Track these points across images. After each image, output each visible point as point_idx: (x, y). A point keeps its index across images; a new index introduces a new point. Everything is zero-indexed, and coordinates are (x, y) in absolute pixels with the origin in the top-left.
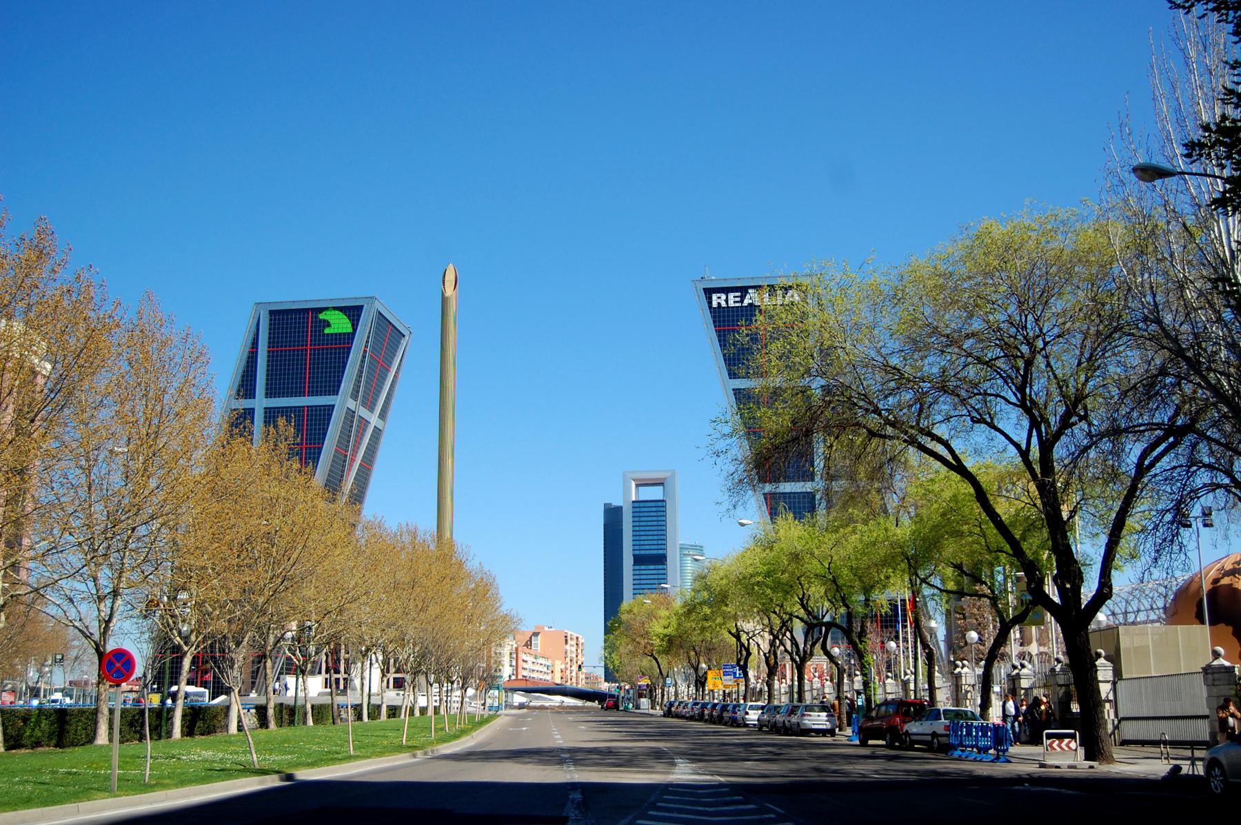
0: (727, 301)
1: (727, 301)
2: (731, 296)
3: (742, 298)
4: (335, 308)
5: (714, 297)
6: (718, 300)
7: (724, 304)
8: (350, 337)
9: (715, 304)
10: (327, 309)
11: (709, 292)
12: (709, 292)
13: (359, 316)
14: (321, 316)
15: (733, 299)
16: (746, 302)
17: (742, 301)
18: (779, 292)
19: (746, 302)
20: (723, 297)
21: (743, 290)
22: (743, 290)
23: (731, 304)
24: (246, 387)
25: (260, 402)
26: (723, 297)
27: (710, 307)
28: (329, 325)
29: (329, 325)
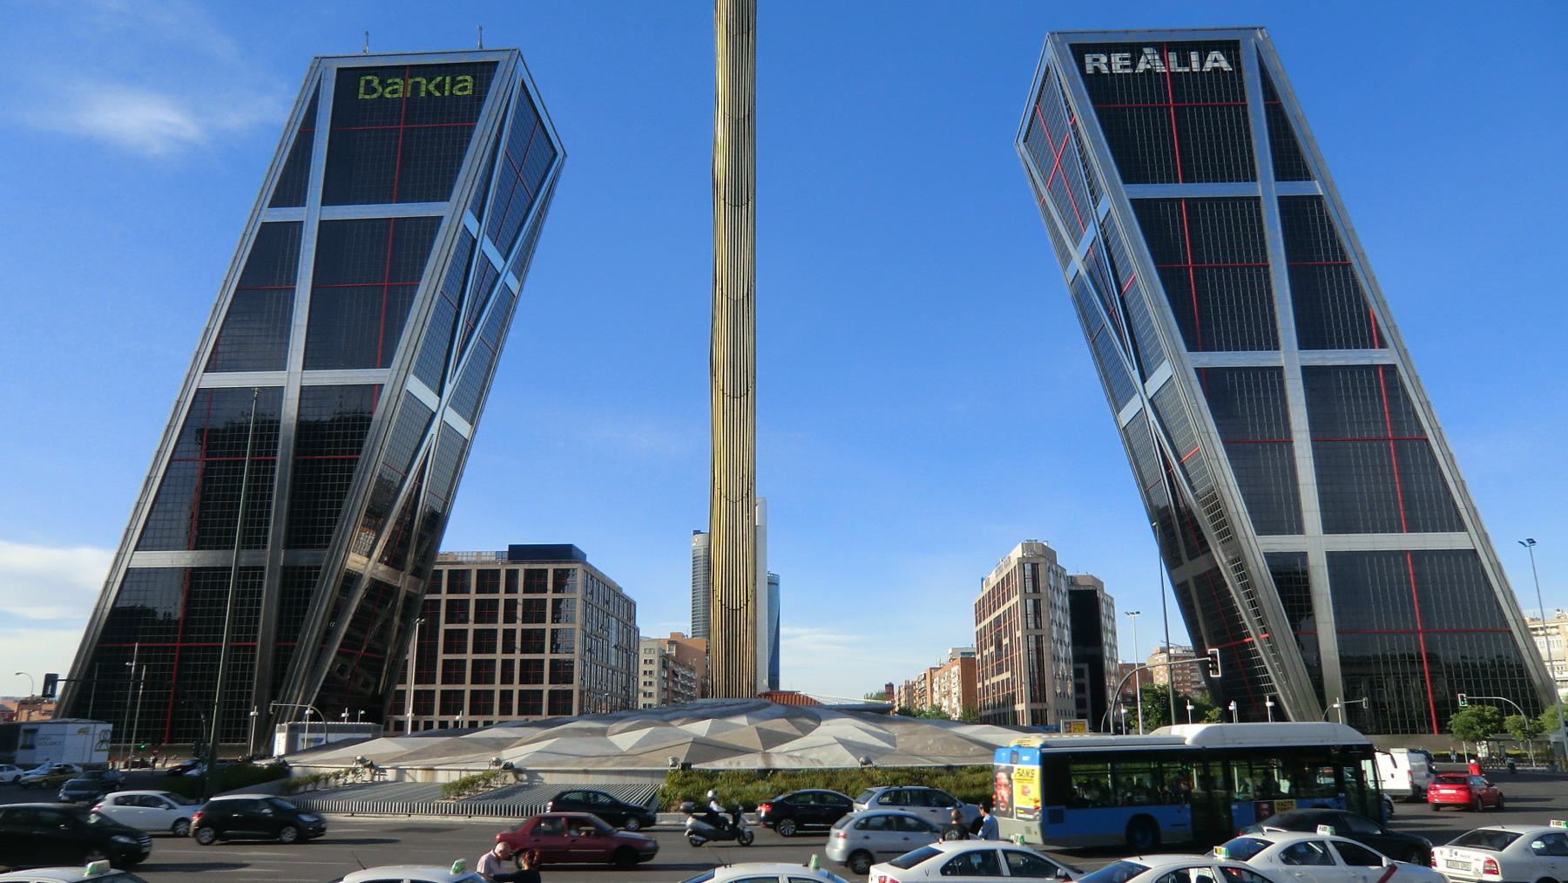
0: (1109, 64)
1: (1109, 64)
2: (1116, 58)
5: (1088, 58)
6: (1096, 62)
7: (1105, 70)
9: (1090, 69)
11: (1079, 51)
13: (490, 79)
15: (1118, 63)
16: (1142, 67)
17: (1134, 66)
18: (1194, 56)
19: (1142, 67)
20: (1104, 59)
21: (1135, 50)
22: (1135, 50)
23: (1117, 69)
24: (289, 189)
25: (311, 214)
26: (1104, 59)
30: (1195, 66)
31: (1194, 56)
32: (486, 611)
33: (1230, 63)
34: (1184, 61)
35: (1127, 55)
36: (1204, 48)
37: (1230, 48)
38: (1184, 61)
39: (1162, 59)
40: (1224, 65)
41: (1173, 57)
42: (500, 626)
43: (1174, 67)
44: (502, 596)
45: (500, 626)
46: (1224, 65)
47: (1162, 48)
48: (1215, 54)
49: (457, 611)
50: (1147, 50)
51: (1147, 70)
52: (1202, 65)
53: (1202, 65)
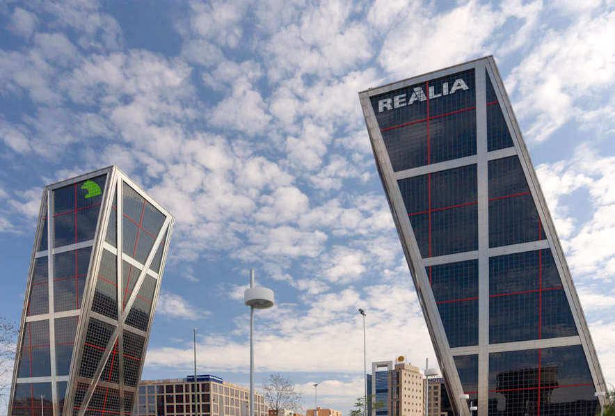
0: (392, 104)
1: (392, 104)
2: (397, 99)
3: (408, 98)
4: (91, 179)
7: (389, 107)
8: (99, 198)
9: (381, 109)
10: (86, 181)
12: (375, 100)
14: (82, 188)
16: (411, 101)
17: (408, 101)
18: (445, 86)
19: (411, 101)
20: (389, 101)
22: (407, 90)
23: (397, 105)
27: (377, 113)
28: (87, 192)
29: (87, 192)
30: (445, 92)
31: (445, 86)
32: (180, 399)
33: (468, 84)
34: (438, 90)
35: (403, 96)
36: (450, 78)
37: (468, 74)
38: (438, 90)
39: (426, 93)
40: (464, 86)
41: (431, 90)
42: (185, 404)
43: (432, 95)
44: (184, 393)
45: (185, 404)
46: (464, 86)
47: (424, 86)
48: (458, 81)
49: (170, 399)
50: (415, 89)
51: (415, 102)
52: (450, 90)
53: (450, 90)
